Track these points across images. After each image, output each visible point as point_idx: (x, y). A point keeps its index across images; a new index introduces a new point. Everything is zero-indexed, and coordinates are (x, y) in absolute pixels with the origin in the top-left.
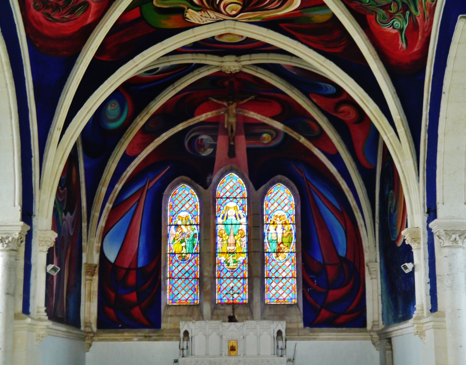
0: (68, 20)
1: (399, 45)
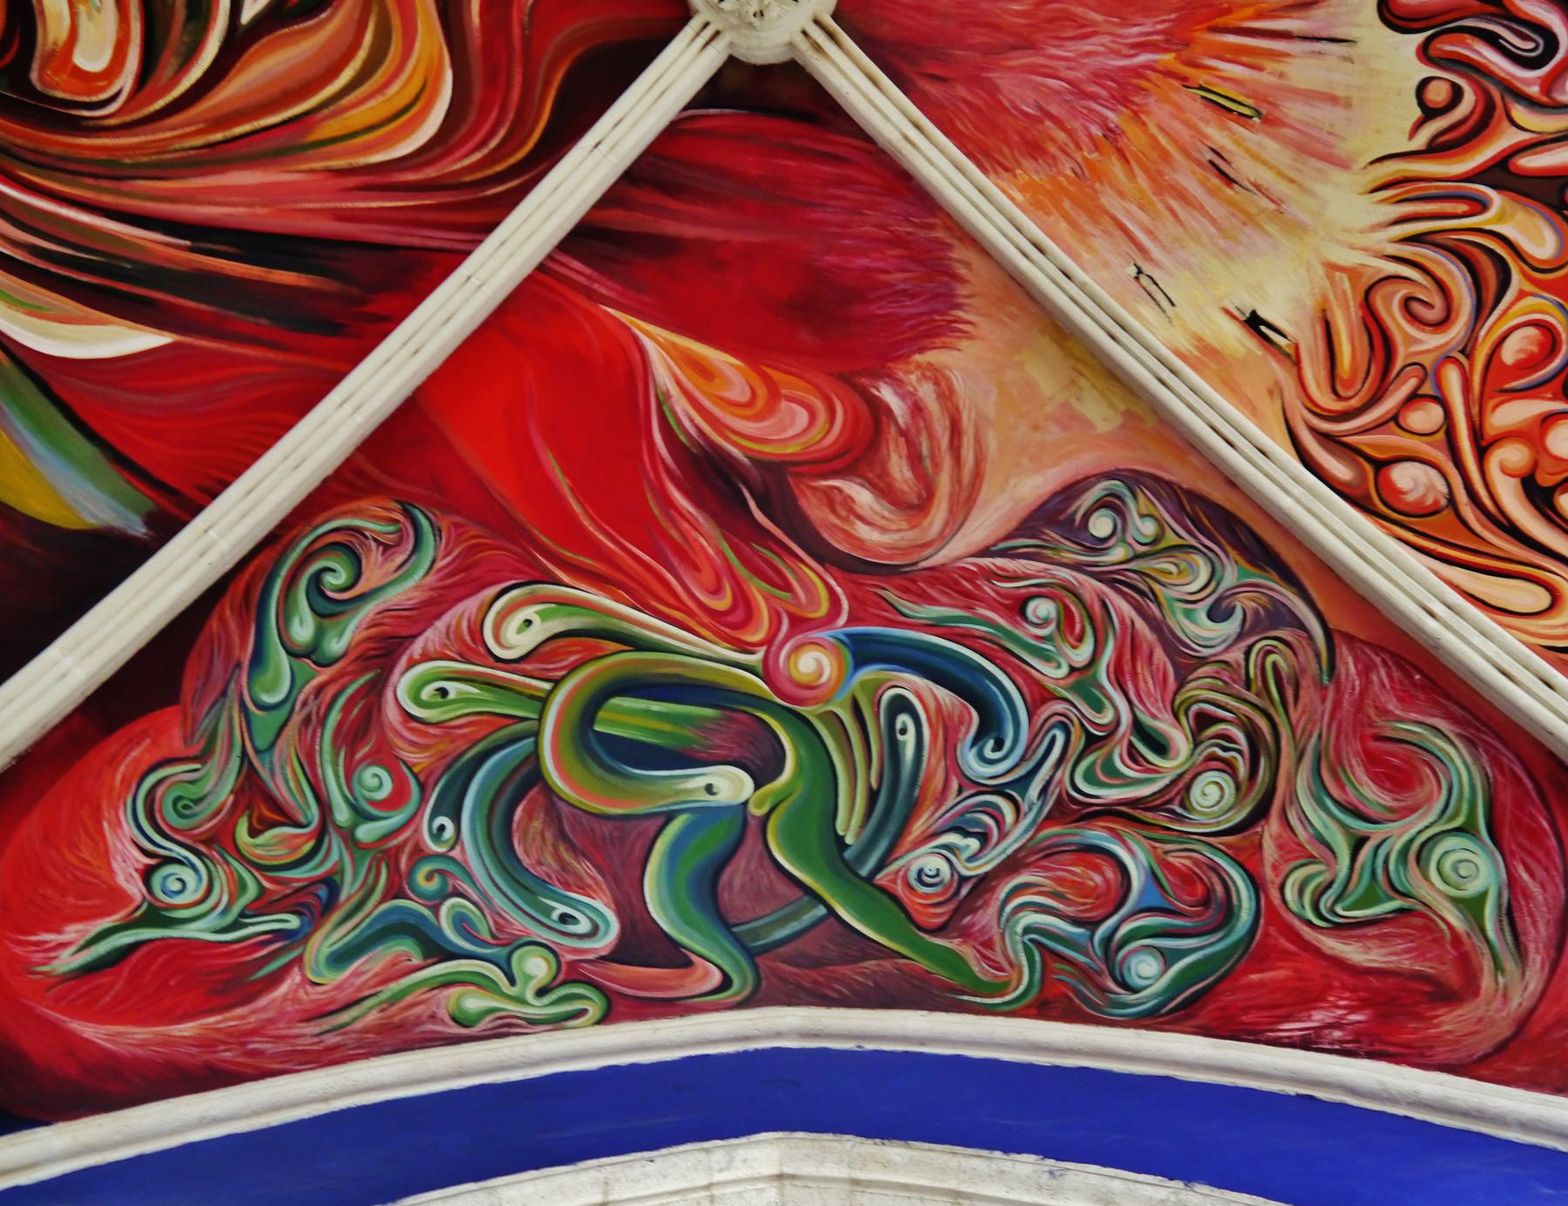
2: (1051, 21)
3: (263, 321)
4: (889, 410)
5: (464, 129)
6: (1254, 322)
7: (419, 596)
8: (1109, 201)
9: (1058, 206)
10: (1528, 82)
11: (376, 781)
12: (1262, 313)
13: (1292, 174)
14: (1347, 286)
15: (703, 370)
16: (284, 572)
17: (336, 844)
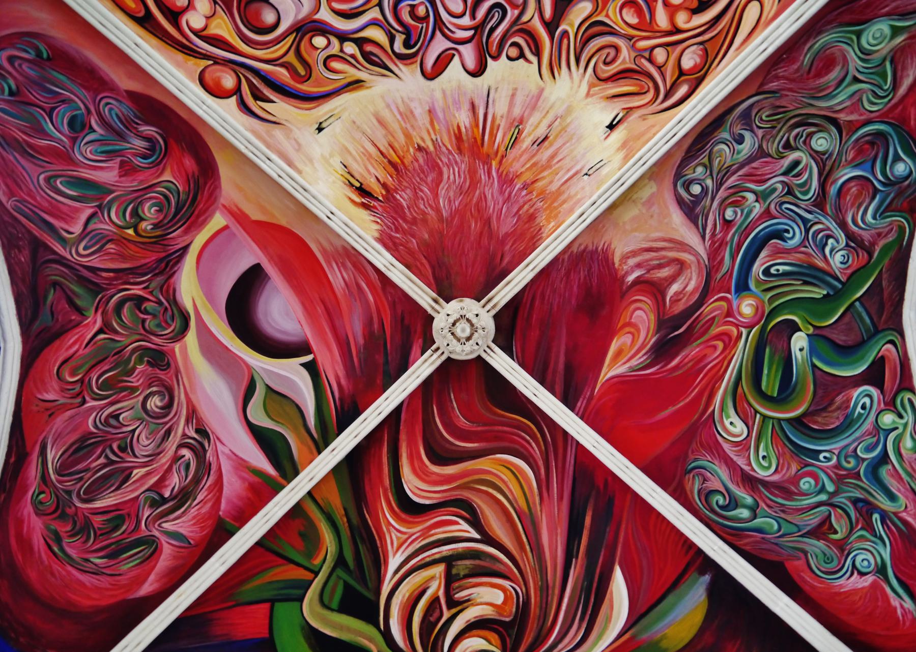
0: (97, 572)
1: (895, 609)
2: (479, 211)
3: (608, 530)
4: (638, 277)
5: (522, 450)
6: (611, 127)
7: (724, 467)
8: (554, 187)
9: (556, 208)
10: (513, 14)
11: (806, 484)
12: (608, 123)
13: (545, 112)
14: (597, 88)
15: (619, 353)
16: (721, 521)
17: (837, 500)
